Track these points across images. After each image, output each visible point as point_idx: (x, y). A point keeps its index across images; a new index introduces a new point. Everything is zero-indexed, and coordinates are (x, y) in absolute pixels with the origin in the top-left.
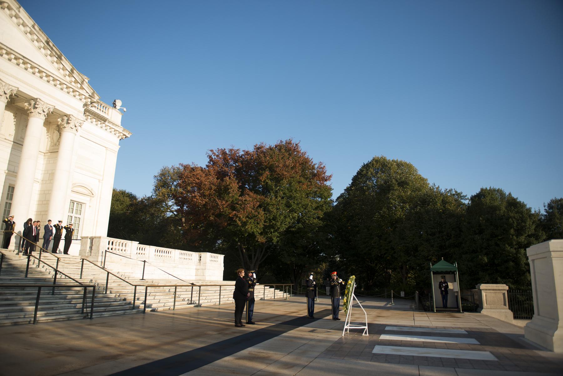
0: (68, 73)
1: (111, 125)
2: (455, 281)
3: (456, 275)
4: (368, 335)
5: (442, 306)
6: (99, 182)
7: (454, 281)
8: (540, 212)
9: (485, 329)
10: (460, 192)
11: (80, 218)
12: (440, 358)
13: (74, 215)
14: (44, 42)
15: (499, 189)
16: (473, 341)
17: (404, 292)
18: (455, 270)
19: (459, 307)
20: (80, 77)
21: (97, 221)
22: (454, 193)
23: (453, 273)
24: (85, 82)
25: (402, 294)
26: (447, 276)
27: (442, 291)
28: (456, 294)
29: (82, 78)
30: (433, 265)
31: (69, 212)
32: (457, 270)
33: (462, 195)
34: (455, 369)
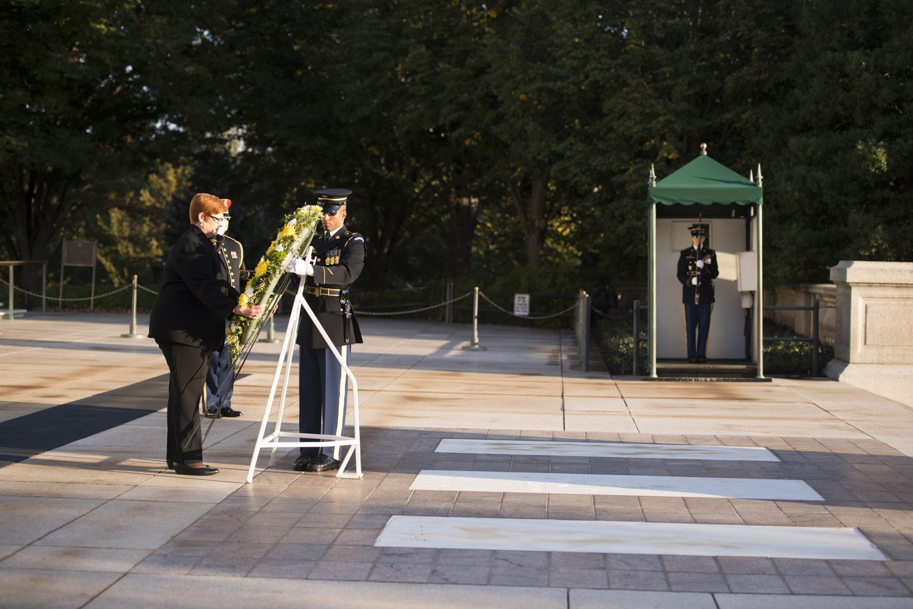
3: (754, 221)
4: (359, 473)
5: (685, 355)
7: (745, 248)
9: (848, 441)
12: (660, 557)
16: (799, 489)
17: (527, 297)
19: (755, 358)
23: (743, 212)
25: (522, 305)
26: (717, 226)
28: (746, 304)
30: (661, 176)
32: (761, 200)
34: (712, 594)
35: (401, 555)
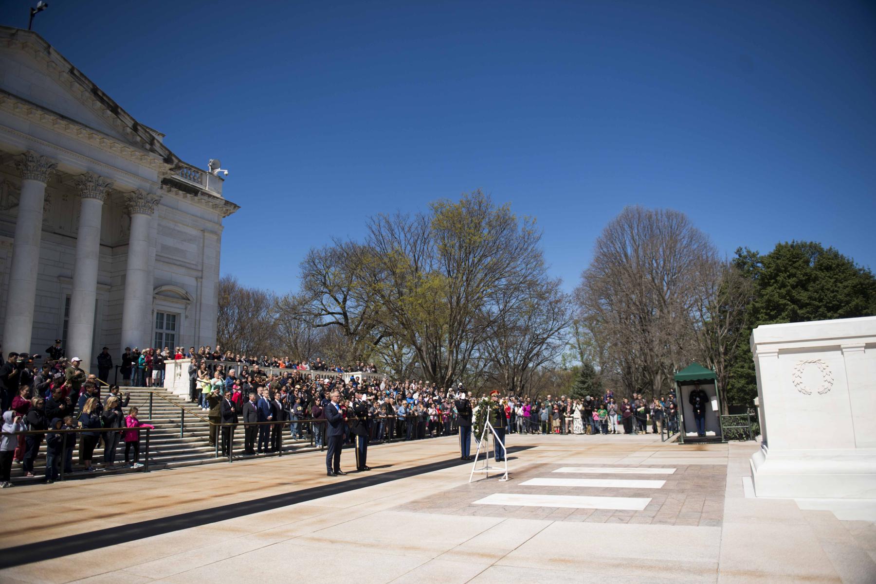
0: (129, 130)
1: (206, 198)
2: (716, 395)
6: (197, 280)
8: (870, 273)
10: (755, 252)
11: (173, 336)
13: (164, 331)
14: (89, 91)
15: (812, 243)
18: (714, 377)
20: (148, 135)
21: (199, 337)
22: (745, 254)
23: (712, 382)
24: (155, 141)
27: (695, 410)
28: (717, 415)
29: (151, 135)
31: (157, 328)
33: (758, 256)
35: (474, 506)
